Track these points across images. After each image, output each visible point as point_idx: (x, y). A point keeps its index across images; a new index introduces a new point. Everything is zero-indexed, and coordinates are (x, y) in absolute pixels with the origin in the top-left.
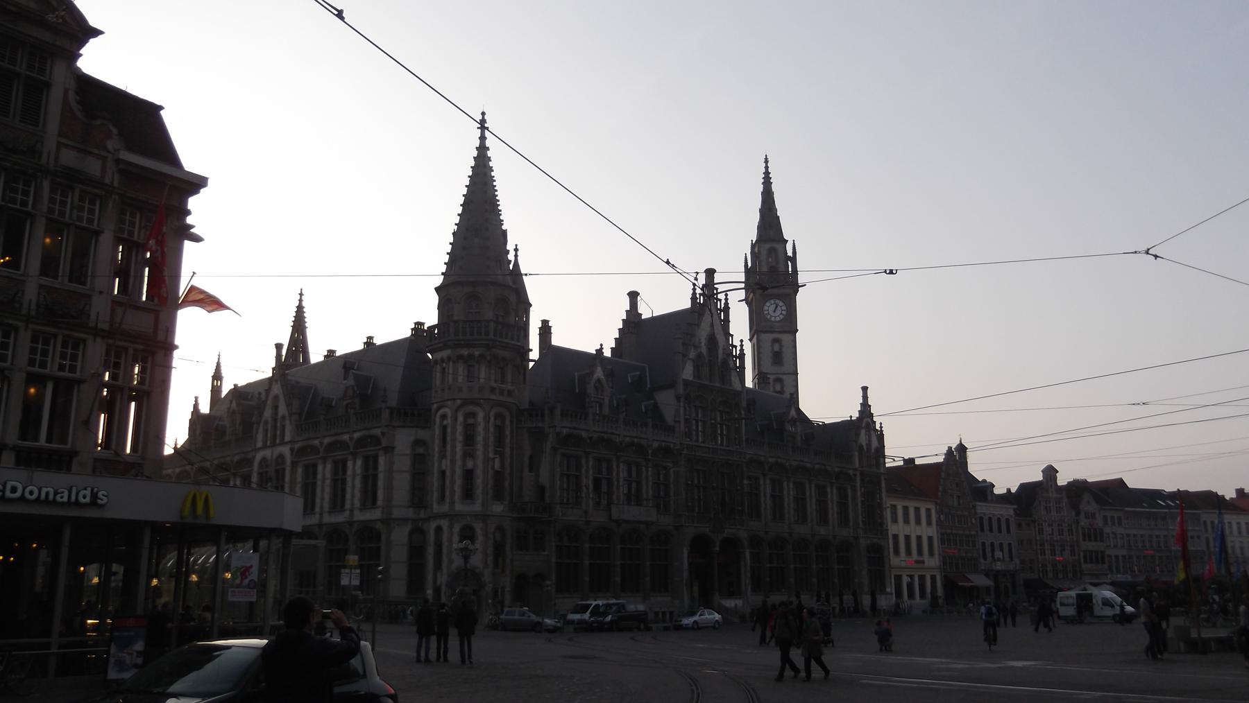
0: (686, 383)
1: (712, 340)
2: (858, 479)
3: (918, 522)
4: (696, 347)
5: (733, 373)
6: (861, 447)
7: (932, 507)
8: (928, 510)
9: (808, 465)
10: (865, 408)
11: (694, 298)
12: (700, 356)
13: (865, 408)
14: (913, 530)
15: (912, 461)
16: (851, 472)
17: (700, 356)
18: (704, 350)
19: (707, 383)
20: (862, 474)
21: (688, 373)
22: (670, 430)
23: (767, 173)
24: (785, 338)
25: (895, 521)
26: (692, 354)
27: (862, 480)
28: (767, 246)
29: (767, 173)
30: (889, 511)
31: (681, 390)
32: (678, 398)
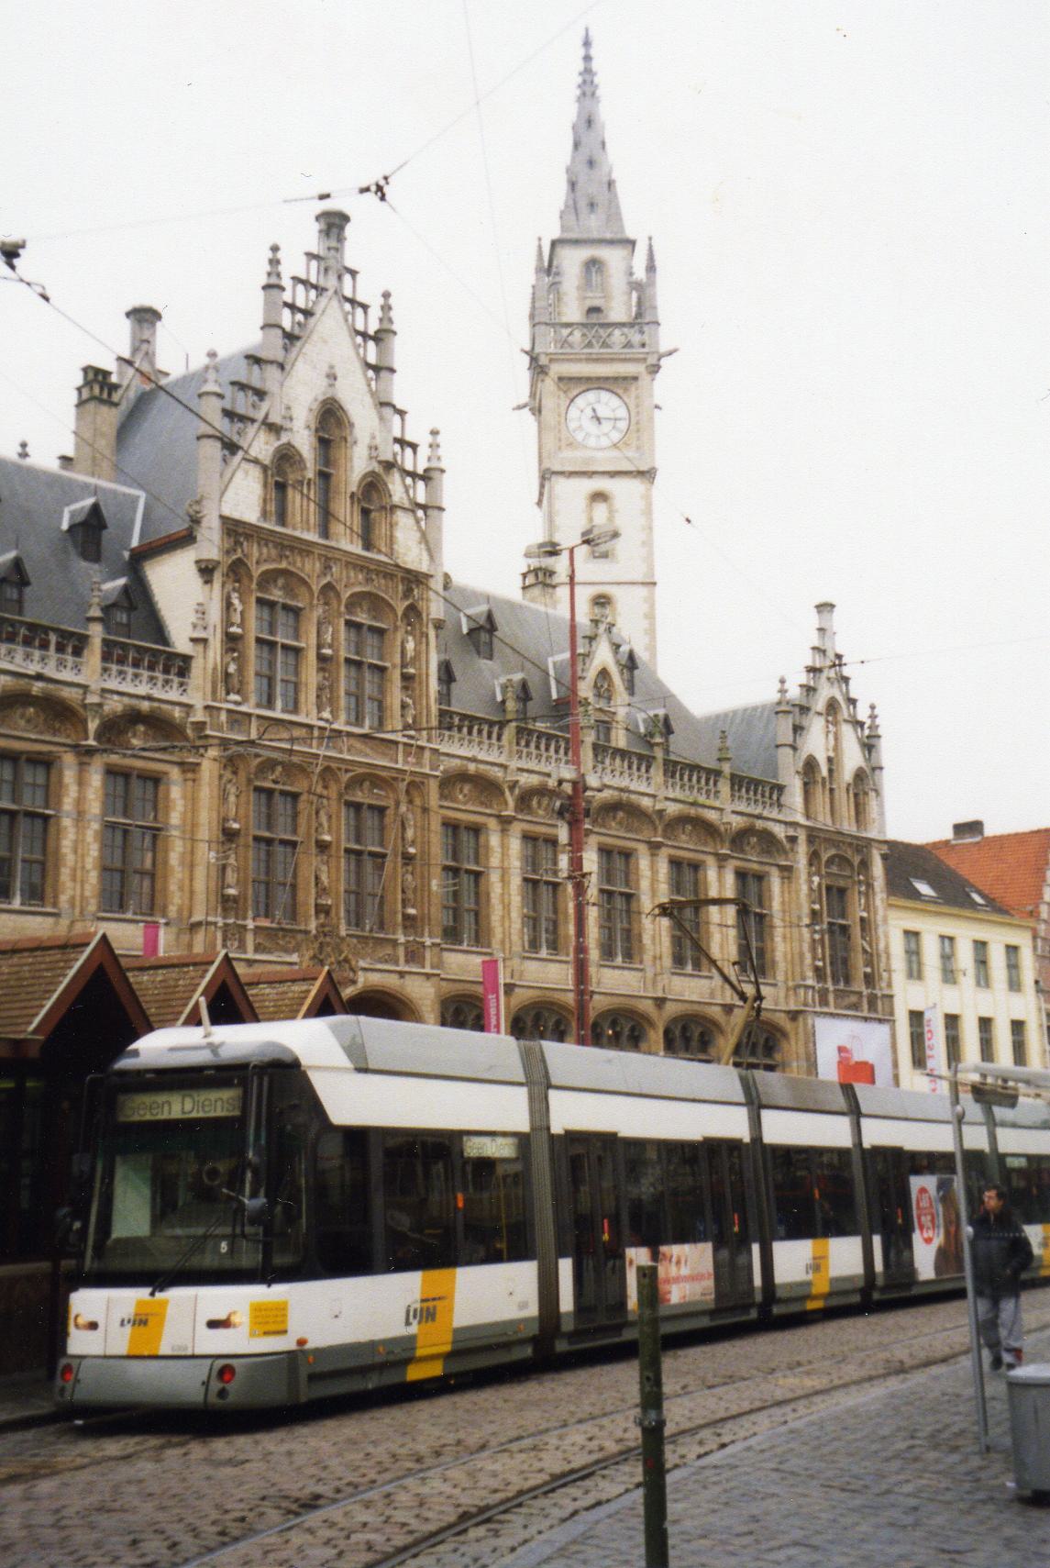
0: (234, 529)
1: (331, 418)
2: (802, 848)
3: (983, 979)
4: (275, 429)
5: (403, 520)
6: (811, 765)
7: (1023, 940)
8: (1012, 950)
9: (646, 803)
10: (826, 665)
11: (272, 287)
12: (286, 457)
13: (826, 665)
14: (969, 1002)
15: (974, 827)
16: (780, 832)
17: (286, 457)
18: (304, 441)
19: (312, 536)
20: (813, 836)
21: (243, 497)
22: (179, 666)
23: (588, 72)
24: (623, 490)
25: (915, 972)
26: (262, 446)
27: (814, 857)
28: (584, 253)
29: (588, 72)
30: (897, 946)
31: (210, 544)
32: (206, 571)
